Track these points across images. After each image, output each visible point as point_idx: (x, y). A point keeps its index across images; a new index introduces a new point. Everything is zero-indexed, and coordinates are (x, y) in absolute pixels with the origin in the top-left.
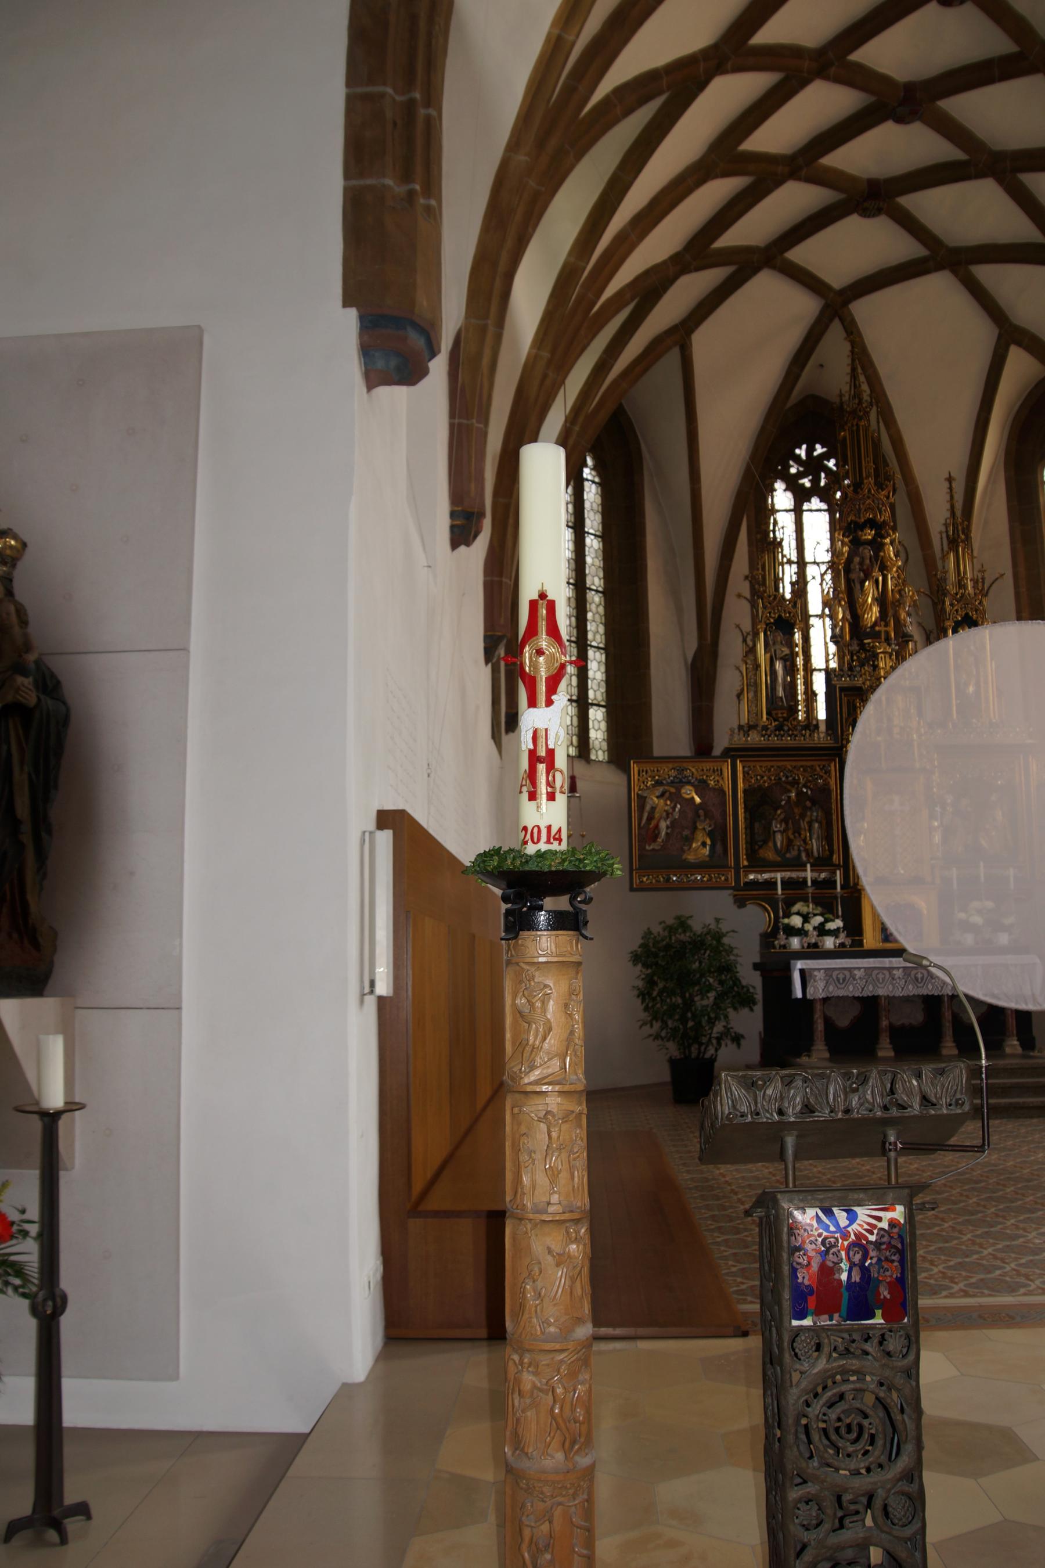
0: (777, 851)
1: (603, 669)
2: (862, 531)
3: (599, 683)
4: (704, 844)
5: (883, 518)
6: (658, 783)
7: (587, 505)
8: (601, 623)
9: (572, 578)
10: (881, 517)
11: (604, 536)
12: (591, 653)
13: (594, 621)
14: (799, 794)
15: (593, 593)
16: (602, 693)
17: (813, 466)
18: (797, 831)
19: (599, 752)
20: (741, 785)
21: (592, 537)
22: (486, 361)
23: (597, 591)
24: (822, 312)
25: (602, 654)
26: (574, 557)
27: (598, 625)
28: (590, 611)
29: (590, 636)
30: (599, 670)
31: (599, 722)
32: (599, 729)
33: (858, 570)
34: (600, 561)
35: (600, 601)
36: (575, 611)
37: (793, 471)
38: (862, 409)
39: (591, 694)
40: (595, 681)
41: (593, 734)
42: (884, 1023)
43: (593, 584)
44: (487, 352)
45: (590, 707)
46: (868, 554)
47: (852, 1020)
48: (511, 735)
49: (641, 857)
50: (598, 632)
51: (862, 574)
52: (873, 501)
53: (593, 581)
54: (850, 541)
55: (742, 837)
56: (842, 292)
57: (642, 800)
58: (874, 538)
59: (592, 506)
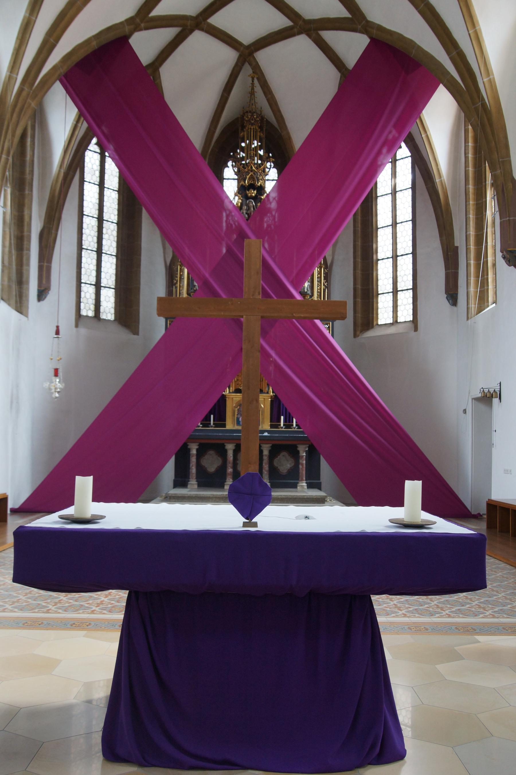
1: (114, 267)
2: (248, 191)
3: (111, 275)
5: (260, 183)
8: (114, 241)
9: (95, 214)
10: (258, 183)
12: (104, 257)
13: (109, 239)
15: (110, 223)
16: (113, 281)
17: (251, 153)
21: (112, 191)
23: (112, 222)
24: (238, 59)
25: (113, 258)
26: (97, 201)
27: (112, 242)
28: (107, 233)
30: (111, 267)
31: (109, 297)
32: (109, 301)
33: (245, 213)
34: (115, 205)
35: (114, 228)
36: (96, 234)
38: (253, 119)
40: (108, 274)
42: (230, 470)
43: (110, 218)
45: (102, 288)
46: (252, 205)
47: (216, 468)
48: (42, 303)
50: (111, 246)
51: (246, 216)
52: (254, 173)
53: (110, 216)
54: (242, 197)
58: (256, 195)
59: (112, 173)
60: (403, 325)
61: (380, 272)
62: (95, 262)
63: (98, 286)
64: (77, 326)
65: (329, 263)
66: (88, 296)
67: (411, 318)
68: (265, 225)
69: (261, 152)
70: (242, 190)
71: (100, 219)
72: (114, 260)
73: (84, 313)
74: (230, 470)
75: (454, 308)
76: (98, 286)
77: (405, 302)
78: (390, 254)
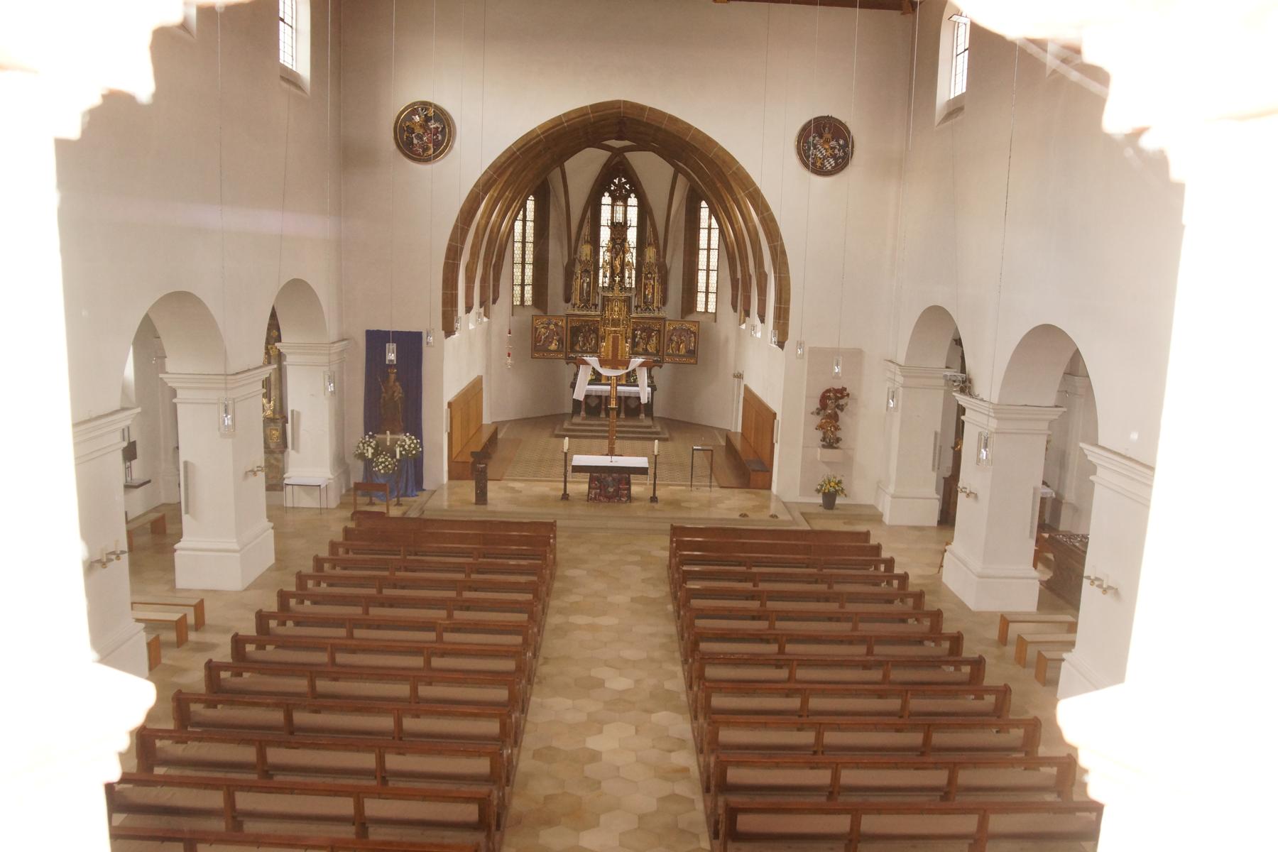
0: (580, 347)
1: (531, 271)
4: (556, 345)
6: (542, 324)
7: (528, 210)
11: (535, 221)
12: (527, 266)
14: (590, 329)
18: (588, 341)
19: (528, 301)
20: (569, 326)
22: (474, 269)
29: (527, 260)
37: (612, 188)
39: (526, 282)
41: (526, 295)
42: (603, 407)
44: (475, 266)
49: (536, 346)
55: (569, 342)
56: (619, 149)
57: (536, 329)
58: (621, 243)
60: (712, 315)
61: (699, 278)
62: (520, 270)
63: (523, 285)
64: (513, 315)
65: (668, 268)
66: (517, 292)
67: (714, 311)
68: (627, 260)
69: (627, 186)
70: (613, 239)
71: (524, 242)
72: (531, 267)
73: (515, 304)
74: (603, 407)
75: (735, 314)
76: (523, 285)
77: (712, 300)
78: (705, 268)
